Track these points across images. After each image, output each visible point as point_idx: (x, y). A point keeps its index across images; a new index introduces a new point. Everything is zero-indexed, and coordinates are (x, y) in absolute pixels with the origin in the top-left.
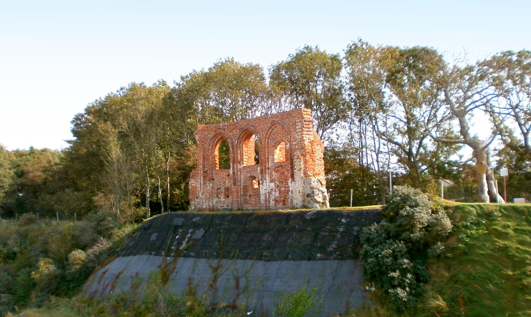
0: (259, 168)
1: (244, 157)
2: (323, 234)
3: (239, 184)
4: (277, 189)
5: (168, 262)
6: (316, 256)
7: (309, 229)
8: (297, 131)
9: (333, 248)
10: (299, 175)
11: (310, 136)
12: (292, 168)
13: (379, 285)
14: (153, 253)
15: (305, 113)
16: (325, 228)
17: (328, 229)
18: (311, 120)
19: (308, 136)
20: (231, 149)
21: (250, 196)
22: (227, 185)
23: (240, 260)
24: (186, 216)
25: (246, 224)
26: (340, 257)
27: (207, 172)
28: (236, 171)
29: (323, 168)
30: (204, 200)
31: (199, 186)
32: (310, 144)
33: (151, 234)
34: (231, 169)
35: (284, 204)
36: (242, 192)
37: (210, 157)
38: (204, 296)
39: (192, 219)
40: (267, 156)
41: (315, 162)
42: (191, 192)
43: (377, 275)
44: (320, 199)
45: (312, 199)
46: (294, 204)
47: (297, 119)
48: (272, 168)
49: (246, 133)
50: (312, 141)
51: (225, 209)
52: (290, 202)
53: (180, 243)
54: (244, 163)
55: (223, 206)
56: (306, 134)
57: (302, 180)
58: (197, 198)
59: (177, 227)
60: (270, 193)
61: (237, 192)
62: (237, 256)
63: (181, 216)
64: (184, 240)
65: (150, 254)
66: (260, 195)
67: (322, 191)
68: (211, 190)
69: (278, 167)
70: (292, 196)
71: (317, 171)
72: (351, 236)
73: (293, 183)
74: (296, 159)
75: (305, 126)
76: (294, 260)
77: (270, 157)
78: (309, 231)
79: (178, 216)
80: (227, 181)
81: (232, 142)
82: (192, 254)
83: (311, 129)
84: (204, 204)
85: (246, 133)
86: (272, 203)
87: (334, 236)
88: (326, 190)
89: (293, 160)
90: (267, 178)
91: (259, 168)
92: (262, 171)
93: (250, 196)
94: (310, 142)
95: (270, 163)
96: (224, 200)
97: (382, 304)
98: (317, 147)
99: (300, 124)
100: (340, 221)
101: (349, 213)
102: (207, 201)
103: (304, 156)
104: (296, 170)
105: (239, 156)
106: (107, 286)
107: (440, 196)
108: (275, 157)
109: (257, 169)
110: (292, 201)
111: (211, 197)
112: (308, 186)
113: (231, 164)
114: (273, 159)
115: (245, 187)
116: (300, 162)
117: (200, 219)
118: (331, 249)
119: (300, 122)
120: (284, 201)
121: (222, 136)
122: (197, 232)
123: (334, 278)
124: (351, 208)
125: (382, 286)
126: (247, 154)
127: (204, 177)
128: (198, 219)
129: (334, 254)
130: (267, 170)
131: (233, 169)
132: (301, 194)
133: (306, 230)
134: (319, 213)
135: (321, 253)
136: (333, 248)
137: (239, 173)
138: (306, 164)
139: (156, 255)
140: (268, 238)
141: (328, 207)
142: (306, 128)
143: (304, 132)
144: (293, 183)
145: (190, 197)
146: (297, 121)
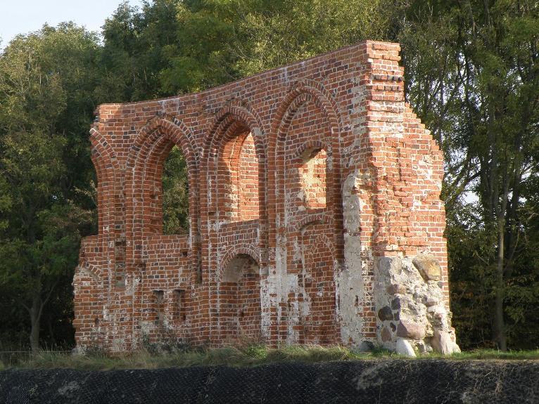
8: (355, 111)
11: (393, 126)
12: (340, 229)
21: (242, 314)
27: (124, 243)
31: (102, 285)
34: (191, 232)
36: (218, 305)
37: (135, 200)
40: (277, 194)
44: (418, 324)
45: (393, 326)
47: (355, 75)
48: (291, 229)
58: (96, 321)
66: (260, 313)
75: (375, 95)
77: (287, 196)
80: (181, 270)
86: (293, 335)
90: (278, 258)
93: (242, 314)
95: (286, 213)
103: (373, 189)
105: (210, 194)
117: (78, 387)
127: (119, 259)
128: (71, 388)
130: (277, 235)
131: (197, 233)
132: (361, 311)
137: (210, 246)
146: (353, 80)
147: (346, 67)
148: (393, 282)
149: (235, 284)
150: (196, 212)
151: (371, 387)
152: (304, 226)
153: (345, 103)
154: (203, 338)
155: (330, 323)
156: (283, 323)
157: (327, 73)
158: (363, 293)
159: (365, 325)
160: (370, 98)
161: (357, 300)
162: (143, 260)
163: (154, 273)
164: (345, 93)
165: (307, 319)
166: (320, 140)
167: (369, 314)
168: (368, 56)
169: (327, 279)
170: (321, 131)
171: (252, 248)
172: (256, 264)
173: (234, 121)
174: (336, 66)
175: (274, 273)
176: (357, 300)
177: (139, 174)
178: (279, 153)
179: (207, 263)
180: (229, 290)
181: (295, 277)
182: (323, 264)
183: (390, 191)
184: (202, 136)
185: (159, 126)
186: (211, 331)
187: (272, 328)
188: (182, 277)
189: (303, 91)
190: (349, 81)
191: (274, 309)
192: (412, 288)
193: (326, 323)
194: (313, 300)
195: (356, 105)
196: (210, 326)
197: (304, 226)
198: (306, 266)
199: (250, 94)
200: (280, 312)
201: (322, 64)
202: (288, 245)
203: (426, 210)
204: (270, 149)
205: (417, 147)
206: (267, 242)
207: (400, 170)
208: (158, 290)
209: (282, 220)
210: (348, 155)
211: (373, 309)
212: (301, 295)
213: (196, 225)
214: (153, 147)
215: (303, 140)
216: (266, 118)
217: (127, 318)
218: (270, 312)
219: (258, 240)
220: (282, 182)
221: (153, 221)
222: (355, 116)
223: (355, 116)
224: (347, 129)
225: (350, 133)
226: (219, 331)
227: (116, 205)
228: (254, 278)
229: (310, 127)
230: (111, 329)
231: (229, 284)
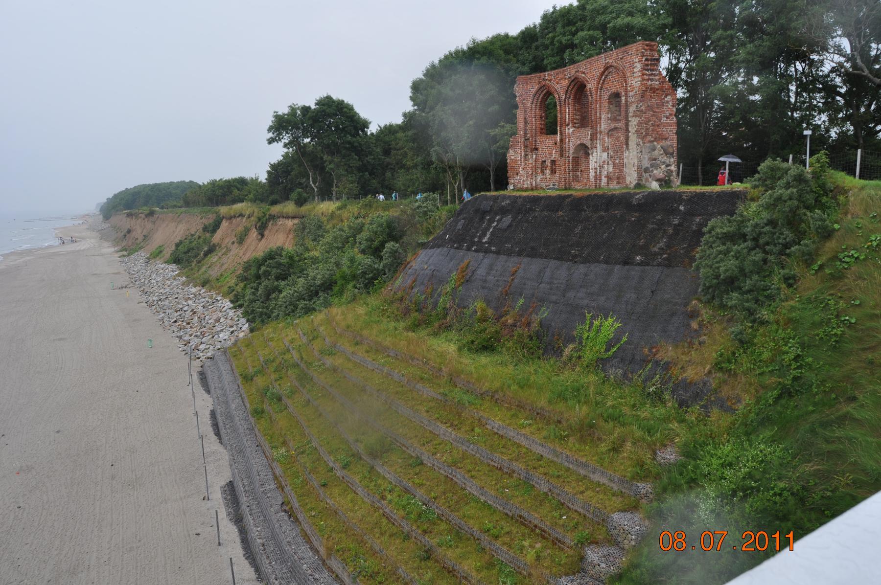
3: (567, 155)
4: (611, 160)
6: (634, 259)
7: (633, 219)
9: (659, 248)
12: (627, 131)
14: (455, 245)
20: (558, 107)
21: (581, 171)
27: (529, 139)
31: (519, 158)
36: (571, 167)
42: (509, 167)
46: (628, 182)
53: (484, 235)
56: (648, 80)
58: (517, 174)
60: (601, 167)
64: (489, 230)
68: (534, 164)
72: (687, 232)
77: (603, 116)
79: (486, 198)
80: (554, 152)
84: (525, 183)
85: (575, 84)
86: (604, 180)
90: (598, 145)
93: (581, 171)
95: (602, 124)
96: (549, 176)
98: (666, 99)
105: (567, 116)
107: (852, 172)
109: (588, 134)
118: (656, 249)
120: (618, 178)
121: (547, 89)
127: (526, 147)
129: (659, 257)
130: (598, 134)
131: (561, 134)
132: (636, 169)
137: (567, 140)
139: (457, 248)
142: (648, 70)
145: (510, 173)
146: (635, 61)
153: (631, 71)
158: (636, 161)
167: (640, 171)
172: (588, 148)
173: (578, 81)
180: (576, 160)
181: (605, 154)
188: (555, 155)
189: (611, 66)
191: (596, 169)
194: (614, 164)
200: (598, 170)
205: (664, 92)
206: (593, 138)
209: (600, 127)
212: (608, 162)
213: (561, 131)
215: (611, 89)
219: (589, 137)
220: (600, 109)
221: (542, 129)
222: (635, 77)
228: (587, 155)
230: (524, 177)
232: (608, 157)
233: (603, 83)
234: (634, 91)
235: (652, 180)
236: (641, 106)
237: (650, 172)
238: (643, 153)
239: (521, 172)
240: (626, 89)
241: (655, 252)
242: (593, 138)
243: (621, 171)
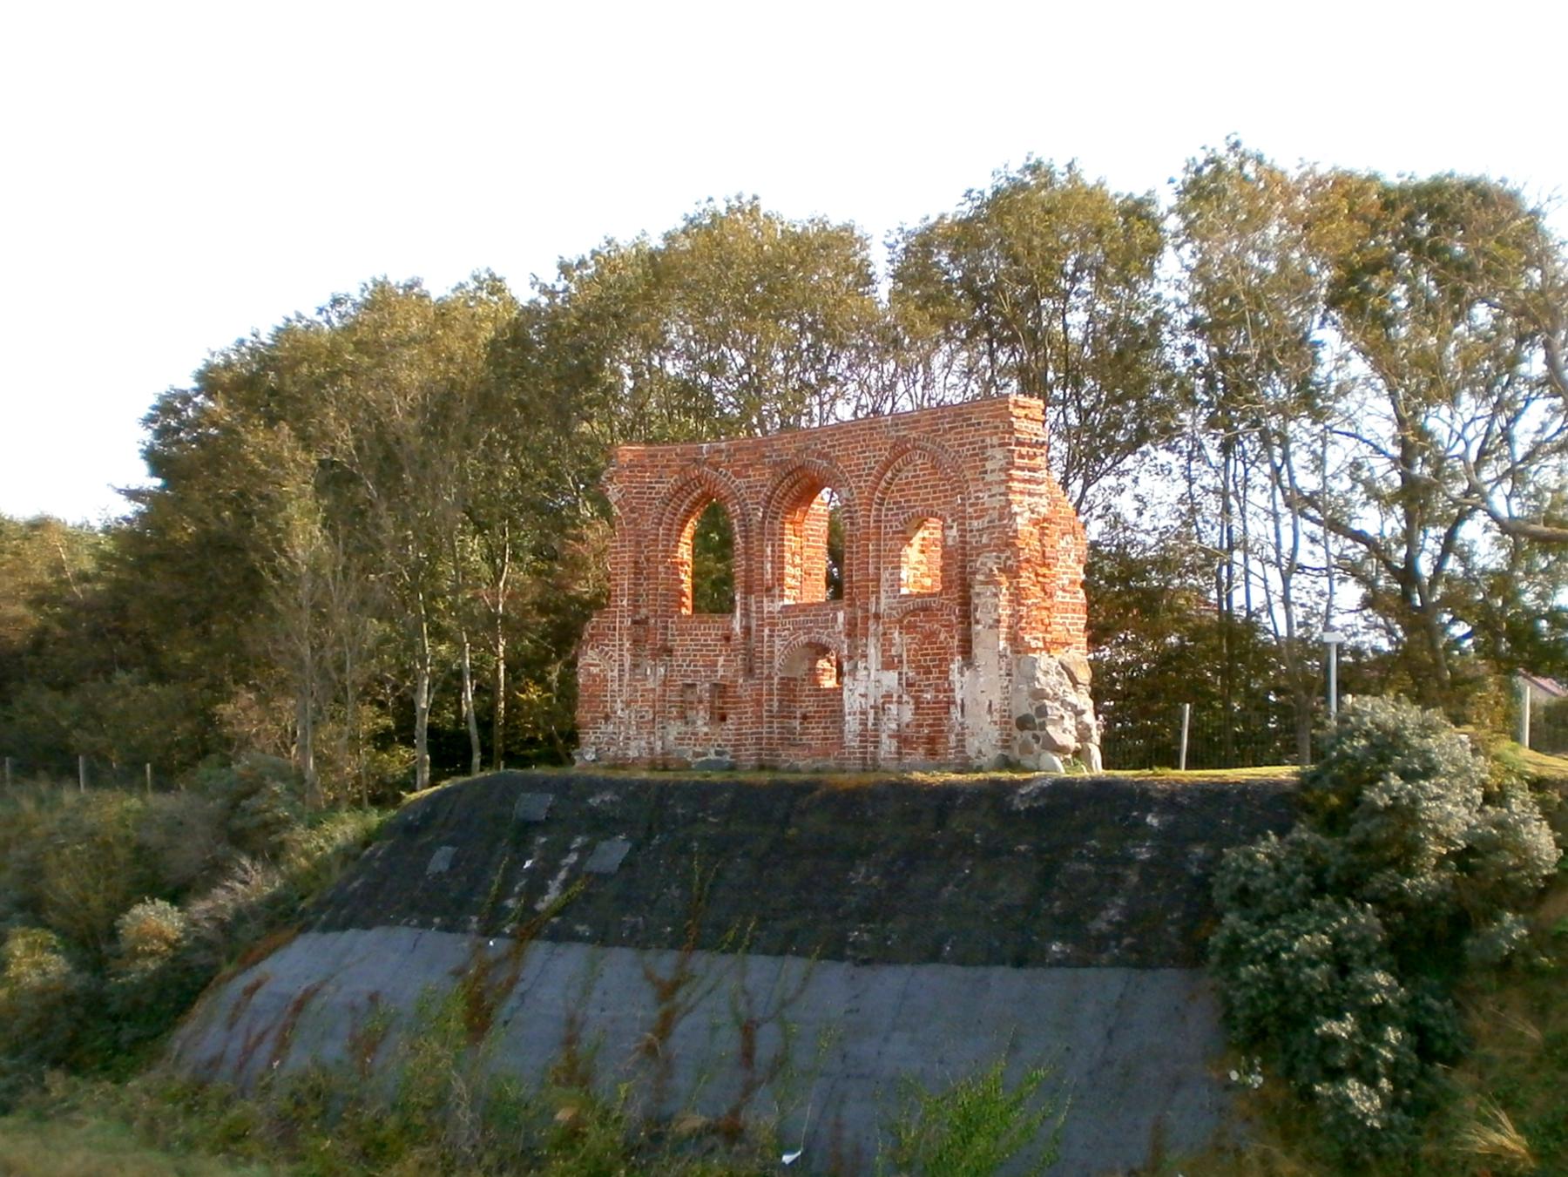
0: (841, 616)
1: (789, 570)
2: (1076, 867)
3: (766, 672)
4: (908, 693)
5: (491, 956)
6: (1044, 951)
7: (1022, 848)
8: (989, 478)
9: (1110, 922)
10: (991, 644)
11: (1036, 499)
12: (967, 617)
13: (1278, 1068)
14: (437, 920)
15: (1022, 413)
16: (1083, 846)
17: (1093, 850)
18: (1041, 439)
19: (1027, 499)
20: (738, 539)
21: (804, 717)
22: (720, 673)
23: (762, 957)
24: (564, 788)
25: (785, 822)
26: (1135, 956)
28: (754, 623)
29: (1081, 620)
30: (632, 732)
31: (616, 673)
32: (1036, 531)
33: (428, 851)
35: (932, 753)
36: (776, 704)
37: (661, 568)
38: (623, 1088)
39: (584, 798)
40: (871, 570)
41: (1051, 596)
42: (583, 696)
43: (1272, 1030)
45: (1037, 738)
46: (971, 752)
47: (991, 435)
48: (890, 616)
49: (796, 482)
50: (1045, 520)
51: (709, 765)
52: (953, 744)
53: (537, 887)
54: (787, 592)
55: (705, 754)
56: (1021, 493)
57: (1003, 664)
58: (607, 718)
59: (528, 827)
60: (880, 710)
61: (759, 703)
62: (752, 938)
63: (545, 785)
64: (553, 876)
65: (425, 924)
66: (843, 717)
67: (1074, 707)
68: (659, 691)
69: (913, 612)
70: (961, 724)
71: (1058, 632)
73: (967, 673)
74: (982, 583)
75: (1018, 461)
76: (962, 962)
77: (885, 575)
78: (1024, 855)
80: (721, 660)
81: (745, 516)
82: (581, 928)
83: (1041, 475)
84: (633, 744)
85: (796, 482)
86: (888, 746)
87: (1117, 879)
88: (1091, 703)
89: (970, 586)
90: (872, 651)
91: (841, 616)
92: (851, 624)
93: (804, 717)
94: (1036, 523)
95: (883, 595)
96: (706, 729)
97: (1289, 1138)
98: (1063, 544)
99: (999, 454)
100: (1139, 823)
101: (1173, 794)
102: (644, 731)
103: (1012, 573)
104: (980, 627)
105: (769, 566)
106: (260, 1039)
108: (903, 575)
109: (835, 619)
110: (961, 743)
111: (660, 716)
112: (1024, 687)
113: (737, 598)
114: (896, 582)
115: (788, 685)
116: (996, 595)
117: (616, 798)
118: (1103, 926)
119: (1001, 445)
120: (931, 740)
121: (706, 488)
122: (604, 846)
123: (1110, 1034)
124: (1183, 774)
125: (1291, 1071)
126: (797, 560)
127: (635, 642)
129: (1113, 943)
130: (871, 622)
131: (746, 614)
132: (996, 717)
133: (1011, 852)
134: (1062, 789)
135: (1063, 938)
136: (1110, 922)
137: (766, 631)
138: (1020, 604)
139: (448, 929)
140: (868, 877)
141: (1095, 768)
142: (1022, 469)
143: (1016, 485)
144: (967, 673)
145: (582, 715)
146: (988, 441)
147: (979, 424)
148: (1038, 686)
149: (795, 679)
150: (746, 587)
151: (1031, 807)
152: (907, 614)
153: (976, 467)
154: (755, 744)
155: (942, 731)
156: (876, 730)
157: (951, 429)
159: (1001, 735)
160: (1012, 463)
161: (990, 705)
162: (669, 644)
163: (684, 661)
164: (977, 455)
165: (908, 726)
166: (936, 509)
167: (1006, 723)
168: (1011, 414)
169: (938, 678)
170: (939, 498)
171: (828, 635)
173: (805, 476)
174: (964, 420)
175: (866, 668)
176: (990, 705)
177: (668, 535)
178: (875, 521)
179: (762, 652)
181: (894, 675)
182: (931, 661)
183: (1032, 576)
184: (759, 492)
185: (697, 477)
186: (764, 735)
187: (860, 735)
190: (983, 441)
191: (864, 713)
192: (1061, 693)
193: (935, 732)
195: (993, 471)
196: (764, 730)
197: (907, 613)
198: (908, 662)
199: (834, 446)
201: (945, 417)
202: (885, 634)
203: (1067, 600)
204: (863, 516)
205: (1059, 524)
206: (854, 630)
207: (1044, 552)
208: (689, 682)
209: (878, 603)
210: (978, 530)
211: (1010, 717)
212: (900, 697)
214: (687, 501)
216: (857, 476)
217: (651, 717)
218: (858, 716)
223: (990, 483)
224: (977, 498)
225: (983, 504)
226: (776, 736)
227: (635, 573)
229: (921, 492)
230: (628, 728)
231: (789, 679)
232: (900, 684)
233: (887, 489)
234: (987, 519)
235: (1044, 747)
236: (1008, 558)
237: (1035, 729)
238: (1014, 678)
239: (619, 712)
240: (964, 512)
241: (1099, 930)
242: (852, 630)
243: (937, 723)
